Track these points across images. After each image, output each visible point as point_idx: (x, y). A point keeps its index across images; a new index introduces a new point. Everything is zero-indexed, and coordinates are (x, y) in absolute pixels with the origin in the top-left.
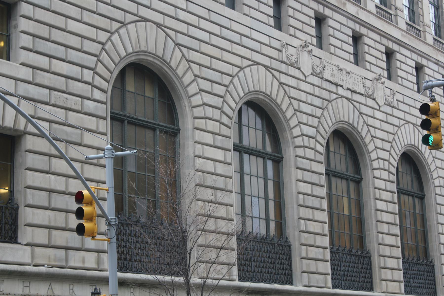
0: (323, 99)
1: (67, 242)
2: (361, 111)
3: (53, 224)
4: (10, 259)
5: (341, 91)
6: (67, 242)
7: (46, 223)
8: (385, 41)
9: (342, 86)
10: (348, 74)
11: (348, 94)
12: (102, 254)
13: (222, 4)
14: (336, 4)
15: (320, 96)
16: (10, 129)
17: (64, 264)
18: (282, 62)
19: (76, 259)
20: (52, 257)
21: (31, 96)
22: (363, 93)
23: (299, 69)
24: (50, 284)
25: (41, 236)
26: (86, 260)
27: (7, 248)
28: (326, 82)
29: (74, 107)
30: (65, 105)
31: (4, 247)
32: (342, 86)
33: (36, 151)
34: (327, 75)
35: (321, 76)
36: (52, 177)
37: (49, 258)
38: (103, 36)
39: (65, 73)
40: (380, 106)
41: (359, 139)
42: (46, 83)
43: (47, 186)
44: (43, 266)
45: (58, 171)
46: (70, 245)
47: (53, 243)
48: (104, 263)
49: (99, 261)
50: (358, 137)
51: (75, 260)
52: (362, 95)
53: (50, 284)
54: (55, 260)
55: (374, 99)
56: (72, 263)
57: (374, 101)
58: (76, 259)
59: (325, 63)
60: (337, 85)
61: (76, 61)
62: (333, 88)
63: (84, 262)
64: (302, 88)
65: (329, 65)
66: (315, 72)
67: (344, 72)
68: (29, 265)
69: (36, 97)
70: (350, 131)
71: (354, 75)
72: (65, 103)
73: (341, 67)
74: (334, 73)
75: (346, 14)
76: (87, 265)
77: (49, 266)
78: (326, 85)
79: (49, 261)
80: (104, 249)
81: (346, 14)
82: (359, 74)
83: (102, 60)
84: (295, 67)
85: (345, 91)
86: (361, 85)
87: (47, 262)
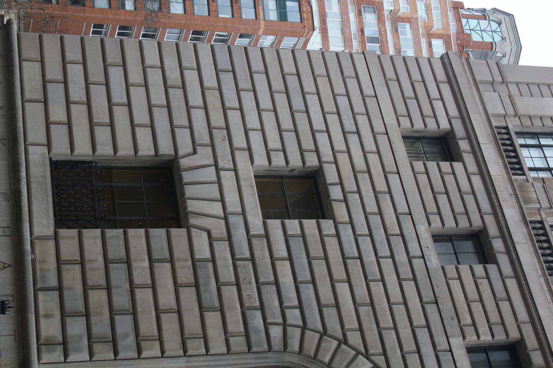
1: (69, 289)
3: (88, 266)
4: (35, 207)
6: (69, 289)
7: (87, 256)
12: (61, 348)
16: (183, 194)
17: (39, 285)
19: (48, 302)
20: (45, 266)
21: (233, 232)
24: (10, 266)
25: (69, 249)
26: (50, 320)
27: (47, 203)
29: (244, 294)
30: (241, 280)
31: (47, 200)
33: (171, 240)
36: (146, 264)
37: (44, 262)
38: (354, 338)
39: (281, 280)
42: (257, 253)
43: (133, 256)
44: (33, 252)
45: (156, 272)
46: (66, 293)
47: (63, 267)
48: (49, 351)
49: (50, 343)
51: (46, 301)
53: (10, 266)
54: (42, 270)
56: (41, 296)
58: (48, 302)
61: (303, 296)
63: (47, 316)
68: (31, 236)
69: (234, 239)
72: (244, 280)
76: (42, 321)
77: (33, 261)
79: (40, 262)
80: (70, 353)
83: (323, 340)
87: (37, 259)
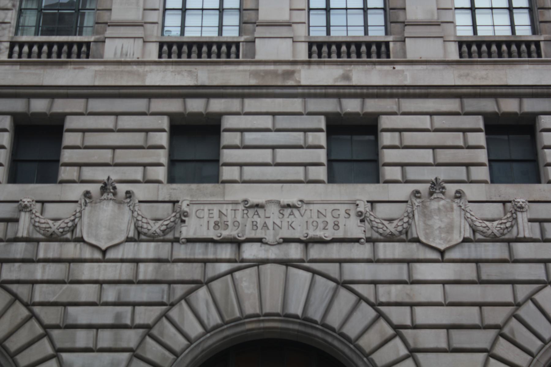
0: (170, 283)
2: (347, 277)
5: (251, 252)
8: (472, 104)
9: (259, 240)
10: (287, 211)
11: (295, 252)
13: (485, 182)
14: (253, 82)
15: (159, 278)
18: (16, 240)
22: (362, 235)
23: (81, 240)
28: (190, 245)
32: (259, 240)
34: (189, 230)
35: (170, 236)
40: (442, 253)
41: (336, 343)
50: (329, 339)
52: (357, 240)
55: (417, 240)
57: (414, 245)
59: (184, 208)
60: (238, 243)
62: (226, 252)
64: (85, 277)
65: (206, 208)
66: (145, 234)
67: (273, 210)
70: (298, 331)
71: (315, 208)
73: (254, 199)
74: (230, 219)
75: (300, 91)
78: (181, 251)
81: (300, 91)
82: (345, 198)
84: (67, 240)
85: (183, 246)
86: (354, 221)
